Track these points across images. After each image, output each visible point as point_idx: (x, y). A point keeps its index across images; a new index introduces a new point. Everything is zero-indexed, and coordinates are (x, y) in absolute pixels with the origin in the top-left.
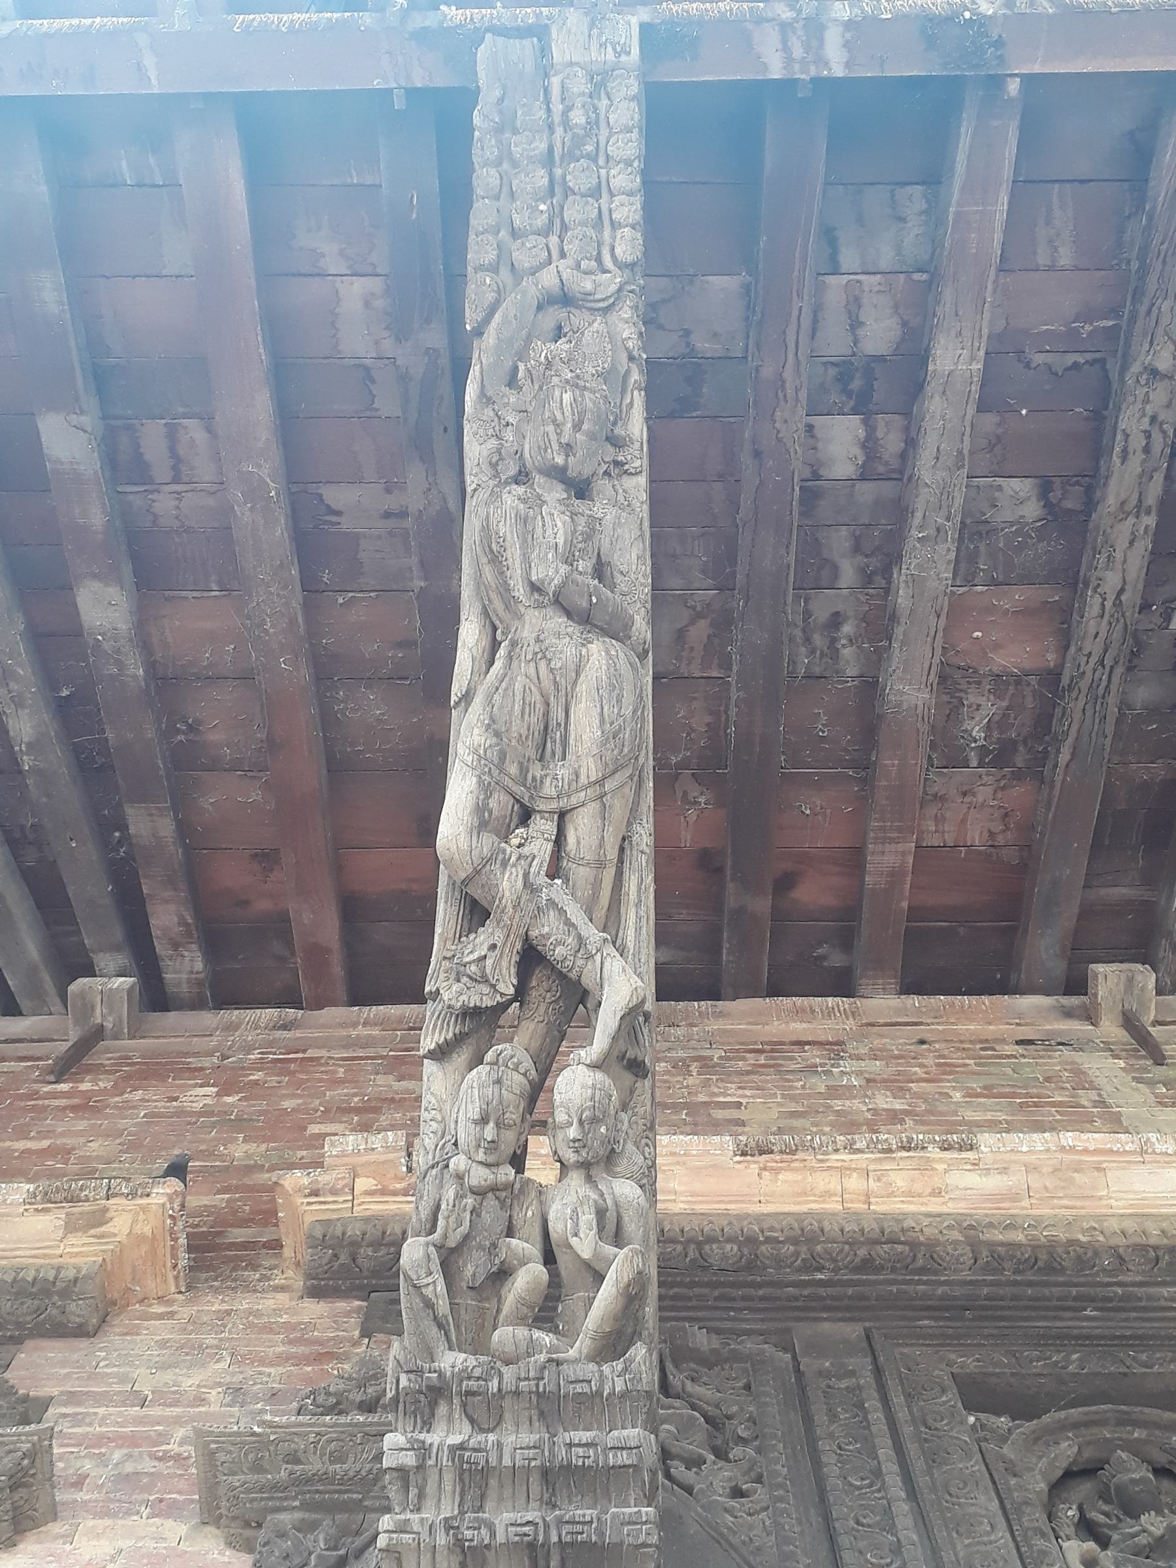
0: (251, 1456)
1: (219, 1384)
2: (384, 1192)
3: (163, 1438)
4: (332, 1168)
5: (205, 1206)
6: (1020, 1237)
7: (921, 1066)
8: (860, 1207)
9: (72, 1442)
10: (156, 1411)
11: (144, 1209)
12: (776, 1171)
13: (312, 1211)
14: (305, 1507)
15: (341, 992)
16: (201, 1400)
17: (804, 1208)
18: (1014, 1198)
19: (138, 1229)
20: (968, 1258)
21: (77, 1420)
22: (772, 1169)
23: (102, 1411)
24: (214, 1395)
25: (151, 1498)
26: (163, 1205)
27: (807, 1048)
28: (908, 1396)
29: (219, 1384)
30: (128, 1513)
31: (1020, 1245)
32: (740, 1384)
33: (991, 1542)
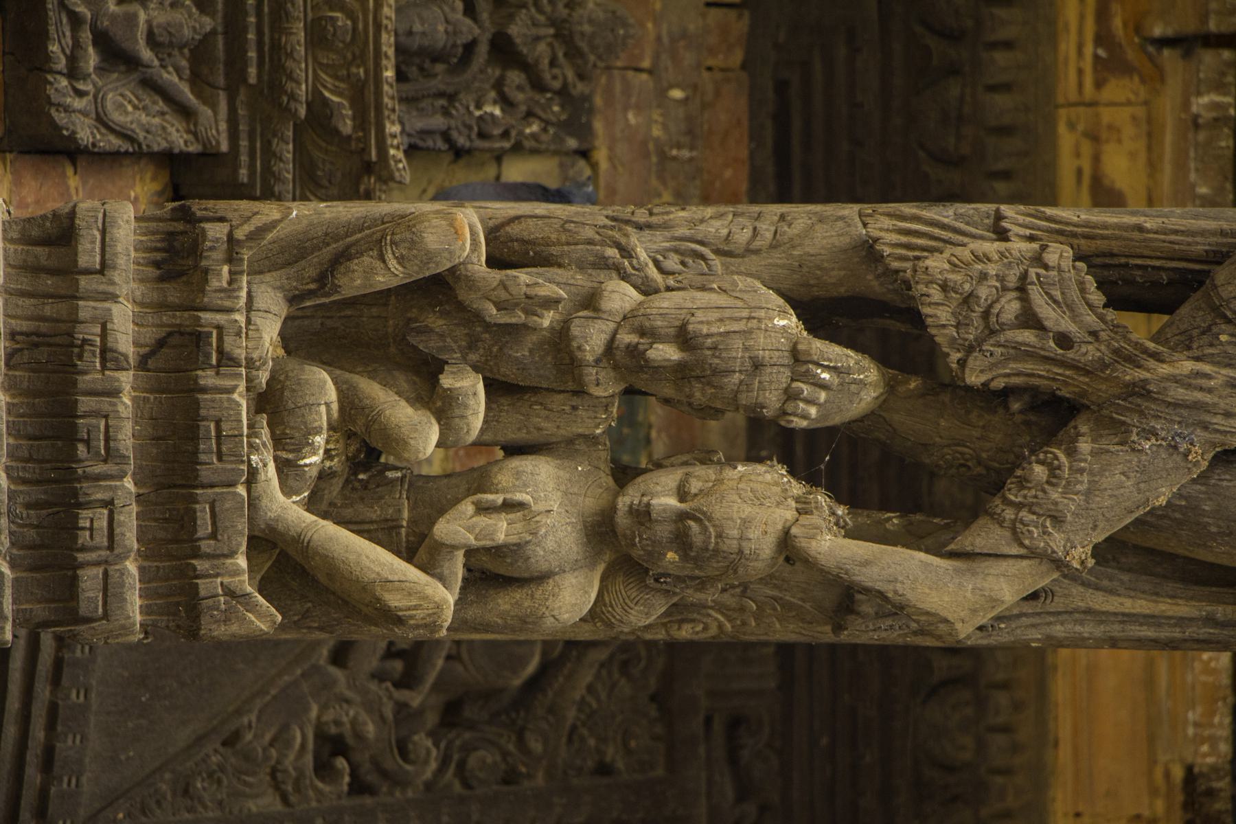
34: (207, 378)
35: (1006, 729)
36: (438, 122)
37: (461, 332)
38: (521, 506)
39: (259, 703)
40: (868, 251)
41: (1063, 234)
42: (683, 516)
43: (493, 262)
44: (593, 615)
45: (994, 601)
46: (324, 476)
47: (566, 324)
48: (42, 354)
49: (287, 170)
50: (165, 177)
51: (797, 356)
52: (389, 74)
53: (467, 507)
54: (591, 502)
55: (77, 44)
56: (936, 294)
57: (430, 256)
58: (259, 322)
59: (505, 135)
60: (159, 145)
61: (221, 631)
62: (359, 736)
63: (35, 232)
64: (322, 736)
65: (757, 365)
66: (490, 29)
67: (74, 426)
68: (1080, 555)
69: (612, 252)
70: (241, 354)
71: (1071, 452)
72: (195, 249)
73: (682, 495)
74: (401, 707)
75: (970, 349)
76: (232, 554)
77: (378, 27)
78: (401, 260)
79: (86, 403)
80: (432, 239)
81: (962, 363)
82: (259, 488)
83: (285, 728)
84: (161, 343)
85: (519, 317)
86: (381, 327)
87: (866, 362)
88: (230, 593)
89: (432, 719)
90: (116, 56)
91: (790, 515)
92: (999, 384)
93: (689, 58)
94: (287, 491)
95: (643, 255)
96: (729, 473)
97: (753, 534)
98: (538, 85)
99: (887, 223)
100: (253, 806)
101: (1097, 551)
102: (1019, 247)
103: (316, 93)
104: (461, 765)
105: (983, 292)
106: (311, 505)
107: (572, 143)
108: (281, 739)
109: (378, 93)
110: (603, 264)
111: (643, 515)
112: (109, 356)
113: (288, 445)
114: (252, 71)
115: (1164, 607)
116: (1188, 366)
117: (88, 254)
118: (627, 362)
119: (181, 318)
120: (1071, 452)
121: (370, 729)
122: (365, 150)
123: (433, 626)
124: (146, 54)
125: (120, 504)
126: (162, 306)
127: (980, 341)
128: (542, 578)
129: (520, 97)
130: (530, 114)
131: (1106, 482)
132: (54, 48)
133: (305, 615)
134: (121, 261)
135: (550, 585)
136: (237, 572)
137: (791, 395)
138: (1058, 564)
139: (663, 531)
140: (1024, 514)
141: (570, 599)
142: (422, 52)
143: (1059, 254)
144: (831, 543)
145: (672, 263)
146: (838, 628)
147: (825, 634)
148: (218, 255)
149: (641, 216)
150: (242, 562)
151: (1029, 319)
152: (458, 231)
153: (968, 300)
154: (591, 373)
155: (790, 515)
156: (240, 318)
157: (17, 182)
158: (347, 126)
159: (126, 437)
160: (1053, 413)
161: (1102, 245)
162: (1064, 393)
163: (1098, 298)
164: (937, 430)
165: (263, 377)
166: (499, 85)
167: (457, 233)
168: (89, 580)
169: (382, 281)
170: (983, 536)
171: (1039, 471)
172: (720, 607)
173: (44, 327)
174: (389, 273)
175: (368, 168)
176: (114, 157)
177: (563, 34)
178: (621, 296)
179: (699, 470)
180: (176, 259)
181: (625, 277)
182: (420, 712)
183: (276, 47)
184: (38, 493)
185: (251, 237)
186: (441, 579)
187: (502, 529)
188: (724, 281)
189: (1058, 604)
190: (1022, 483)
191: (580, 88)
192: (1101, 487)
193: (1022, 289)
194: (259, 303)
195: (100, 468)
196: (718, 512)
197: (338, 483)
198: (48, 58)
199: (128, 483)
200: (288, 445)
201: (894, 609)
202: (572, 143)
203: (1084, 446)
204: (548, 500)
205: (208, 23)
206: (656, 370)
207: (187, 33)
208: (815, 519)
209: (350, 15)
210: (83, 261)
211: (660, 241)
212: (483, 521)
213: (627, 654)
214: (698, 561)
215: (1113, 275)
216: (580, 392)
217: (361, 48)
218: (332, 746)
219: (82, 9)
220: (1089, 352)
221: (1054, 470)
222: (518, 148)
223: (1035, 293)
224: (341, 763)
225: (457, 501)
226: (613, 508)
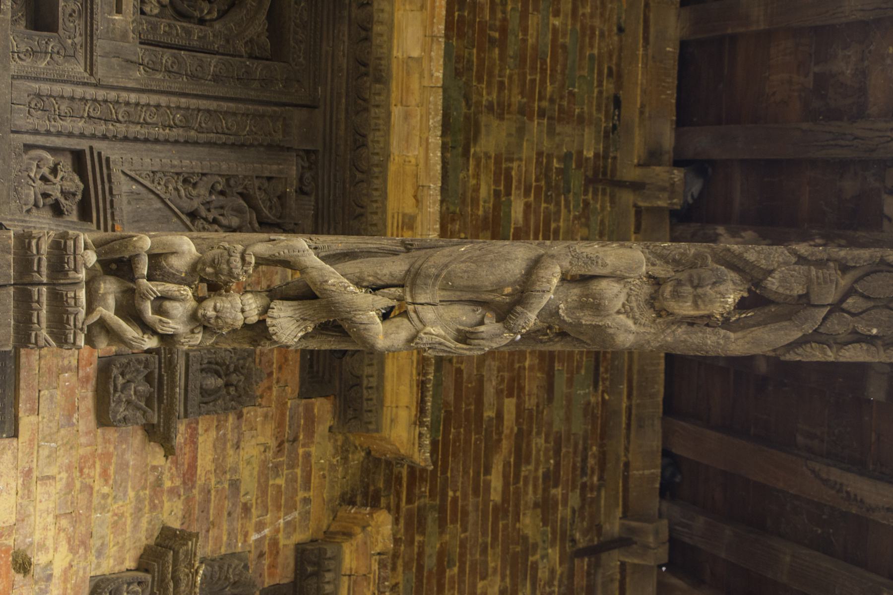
7: (592, 16)
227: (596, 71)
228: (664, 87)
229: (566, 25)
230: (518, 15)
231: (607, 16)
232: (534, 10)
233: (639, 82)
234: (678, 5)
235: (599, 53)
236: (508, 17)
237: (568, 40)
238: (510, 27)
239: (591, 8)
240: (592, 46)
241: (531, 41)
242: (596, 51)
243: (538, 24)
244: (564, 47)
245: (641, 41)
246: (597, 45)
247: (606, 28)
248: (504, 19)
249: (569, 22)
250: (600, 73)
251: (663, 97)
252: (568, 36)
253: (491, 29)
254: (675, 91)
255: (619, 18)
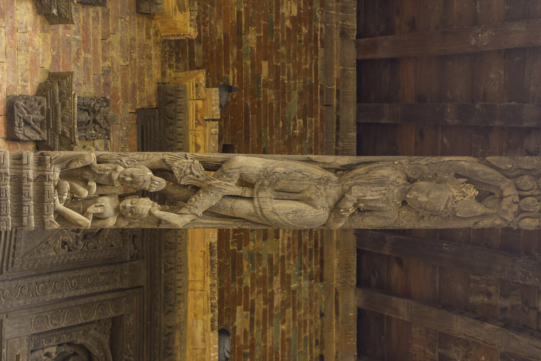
0: (65, 91)
1: (113, 64)
2: (197, 111)
3: (87, 50)
4: (206, 91)
5: (217, 31)
6: (177, 343)
7: (304, 314)
8: (190, 286)
9: (85, 20)
10: (100, 45)
11: (186, 25)
12: (203, 257)
13: (190, 84)
14: (48, 110)
15: (361, 57)
16: (105, 59)
17: (189, 266)
18: (193, 343)
19: (178, 23)
20: (168, 324)
21: (95, 19)
22: (204, 256)
23: (100, 26)
24: (108, 63)
25: (60, 54)
26: (187, 32)
27: (318, 266)
28: (113, 300)
29: (113, 64)
30: (54, 48)
31: (173, 343)
32: (113, 243)
33: (48, 323)
34: (46, 183)
35: (180, 237)
36: (84, 134)
37: (92, 175)
38: (103, 206)
39: (52, 236)
40: (164, 161)
41: (197, 158)
42: (132, 207)
43: (98, 163)
44: (115, 224)
45: (186, 222)
46: (67, 200)
47: (111, 173)
48: (16, 179)
49: (57, 143)
50: (35, 144)
51: (152, 179)
52: (76, 127)
53: (93, 206)
54: (115, 205)
55: (20, 122)
56: (176, 169)
57: (87, 162)
58: (55, 173)
59: (95, 136)
60: (35, 139)
61: (49, 228)
62: (69, 242)
63: (15, 158)
64: (62, 241)
65: (145, 181)
66: (93, 118)
67: (22, 192)
68: (200, 214)
69: (119, 161)
70: (52, 179)
71: (199, 196)
72: (44, 160)
73: (132, 204)
74: (76, 236)
75: (182, 178)
76: (51, 215)
77: (74, 118)
78: (81, 162)
79: (24, 188)
80: (87, 159)
81: (180, 180)
82: (55, 203)
83: (56, 241)
84: (38, 177)
85: (102, 172)
86: (76, 174)
87: (164, 180)
88: (50, 221)
89: (82, 238)
90: (27, 123)
91: (150, 207)
92: (186, 184)
93: (127, 122)
94: (60, 203)
95: (124, 162)
96: (140, 200)
97: (144, 210)
98: (101, 127)
99: (167, 156)
100: (51, 254)
101: (203, 213)
102: (190, 160)
103: (63, 130)
104: (87, 246)
105: (184, 168)
106: (64, 205)
107: (107, 137)
108: (55, 242)
109: (74, 130)
110: (117, 163)
111: (124, 207)
112: (29, 180)
113: (61, 195)
114: (51, 126)
115: (214, 222)
116: (218, 181)
117: (25, 161)
118: (122, 181)
119: (41, 173)
120: (199, 196)
121: (71, 240)
122: (72, 140)
123: (87, 227)
124: (32, 123)
125: (30, 206)
126: (38, 171)
127: (183, 177)
128: (106, 218)
129: (98, 129)
130: (100, 132)
131: (205, 201)
132: (16, 122)
133: (63, 224)
134: (31, 163)
135: (108, 219)
136: (52, 218)
137: (151, 186)
138: (196, 215)
139: (128, 210)
140: (191, 207)
141: (111, 222)
142: (81, 122)
143: (197, 162)
144: (158, 212)
145: (129, 162)
146: (158, 226)
147: (156, 227)
148: (48, 162)
149: (124, 154)
150: (53, 216)
151: (192, 173)
152: (91, 157)
153: (181, 170)
154: (115, 182)
155: (150, 207)
156: (52, 173)
157: (9, 146)
158: (68, 136)
159: (31, 194)
160: (196, 189)
161: (204, 160)
162: (198, 186)
163: (203, 169)
164: (176, 192)
165: (56, 183)
166: (94, 127)
167: (92, 158)
168: (25, 219)
169: (78, 166)
170: (184, 211)
171: (193, 199)
172: (137, 223)
173: (17, 174)
174: (80, 165)
175: (72, 143)
176: (26, 141)
177: (105, 118)
178: (121, 169)
179: (134, 199)
180: (41, 162)
181: (121, 165)
182: (80, 237)
183: (56, 122)
184: (15, 204)
185: (54, 158)
186: (88, 218)
187: (99, 210)
188: (139, 166)
189: (196, 221)
190: (191, 201)
191: (108, 128)
192: (204, 202)
193: (190, 168)
194: (56, 170)
195: (27, 199)
196: (138, 207)
197: (69, 201)
198: (15, 124)
199: (32, 202)
200: (61, 195)
201: (167, 222)
202: (107, 137)
203: (201, 195)
204: (107, 205)
205: (43, 118)
206: (127, 182)
207: (40, 119)
208: (155, 208)
209: (69, 116)
210: (24, 163)
211: (127, 158)
212: (96, 208)
213: (123, 231)
214: (134, 215)
215: (205, 165)
216: (113, 185)
217: (71, 122)
218: (64, 243)
219: (21, 116)
220: (202, 179)
221: (196, 199)
222: (98, 138)
223: (193, 168)
224: (66, 246)
225: (91, 205)
226: (119, 206)
227: (308, 345)
228: (349, 337)
229: (290, 326)
230: (260, 333)
231: (313, 310)
232: (270, 326)
233: (334, 340)
234: (355, 287)
235: (310, 334)
236: (255, 336)
237: (291, 334)
238: (256, 342)
239: (304, 310)
240: (305, 332)
241: (268, 345)
242: (308, 334)
243: (273, 333)
244: (289, 340)
245: (334, 315)
246: (308, 330)
247: (313, 318)
248: (253, 339)
249: (291, 324)
250: (311, 346)
251: (349, 343)
252: (291, 332)
253: (245, 349)
254: (356, 338)
255: (321, 308)
